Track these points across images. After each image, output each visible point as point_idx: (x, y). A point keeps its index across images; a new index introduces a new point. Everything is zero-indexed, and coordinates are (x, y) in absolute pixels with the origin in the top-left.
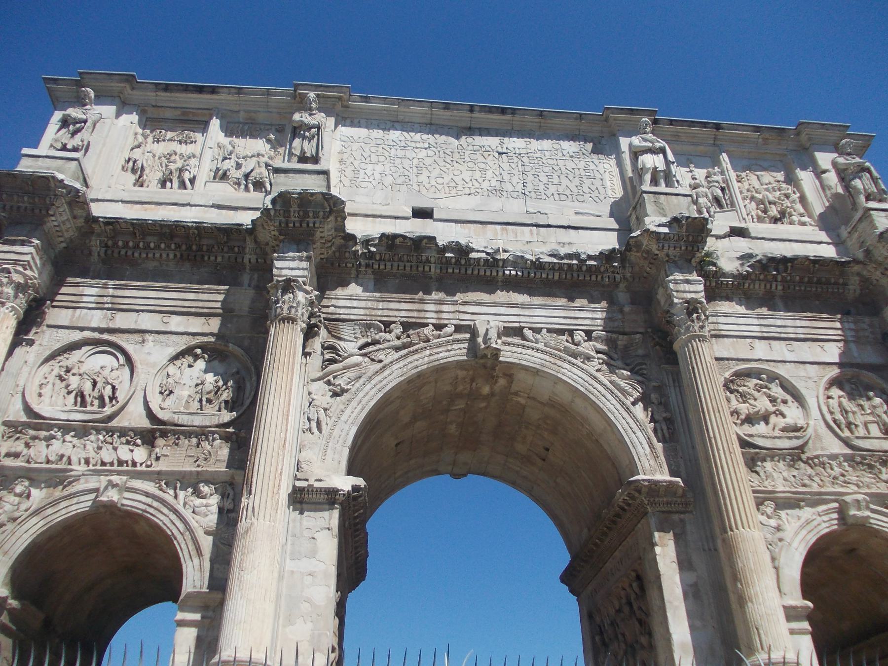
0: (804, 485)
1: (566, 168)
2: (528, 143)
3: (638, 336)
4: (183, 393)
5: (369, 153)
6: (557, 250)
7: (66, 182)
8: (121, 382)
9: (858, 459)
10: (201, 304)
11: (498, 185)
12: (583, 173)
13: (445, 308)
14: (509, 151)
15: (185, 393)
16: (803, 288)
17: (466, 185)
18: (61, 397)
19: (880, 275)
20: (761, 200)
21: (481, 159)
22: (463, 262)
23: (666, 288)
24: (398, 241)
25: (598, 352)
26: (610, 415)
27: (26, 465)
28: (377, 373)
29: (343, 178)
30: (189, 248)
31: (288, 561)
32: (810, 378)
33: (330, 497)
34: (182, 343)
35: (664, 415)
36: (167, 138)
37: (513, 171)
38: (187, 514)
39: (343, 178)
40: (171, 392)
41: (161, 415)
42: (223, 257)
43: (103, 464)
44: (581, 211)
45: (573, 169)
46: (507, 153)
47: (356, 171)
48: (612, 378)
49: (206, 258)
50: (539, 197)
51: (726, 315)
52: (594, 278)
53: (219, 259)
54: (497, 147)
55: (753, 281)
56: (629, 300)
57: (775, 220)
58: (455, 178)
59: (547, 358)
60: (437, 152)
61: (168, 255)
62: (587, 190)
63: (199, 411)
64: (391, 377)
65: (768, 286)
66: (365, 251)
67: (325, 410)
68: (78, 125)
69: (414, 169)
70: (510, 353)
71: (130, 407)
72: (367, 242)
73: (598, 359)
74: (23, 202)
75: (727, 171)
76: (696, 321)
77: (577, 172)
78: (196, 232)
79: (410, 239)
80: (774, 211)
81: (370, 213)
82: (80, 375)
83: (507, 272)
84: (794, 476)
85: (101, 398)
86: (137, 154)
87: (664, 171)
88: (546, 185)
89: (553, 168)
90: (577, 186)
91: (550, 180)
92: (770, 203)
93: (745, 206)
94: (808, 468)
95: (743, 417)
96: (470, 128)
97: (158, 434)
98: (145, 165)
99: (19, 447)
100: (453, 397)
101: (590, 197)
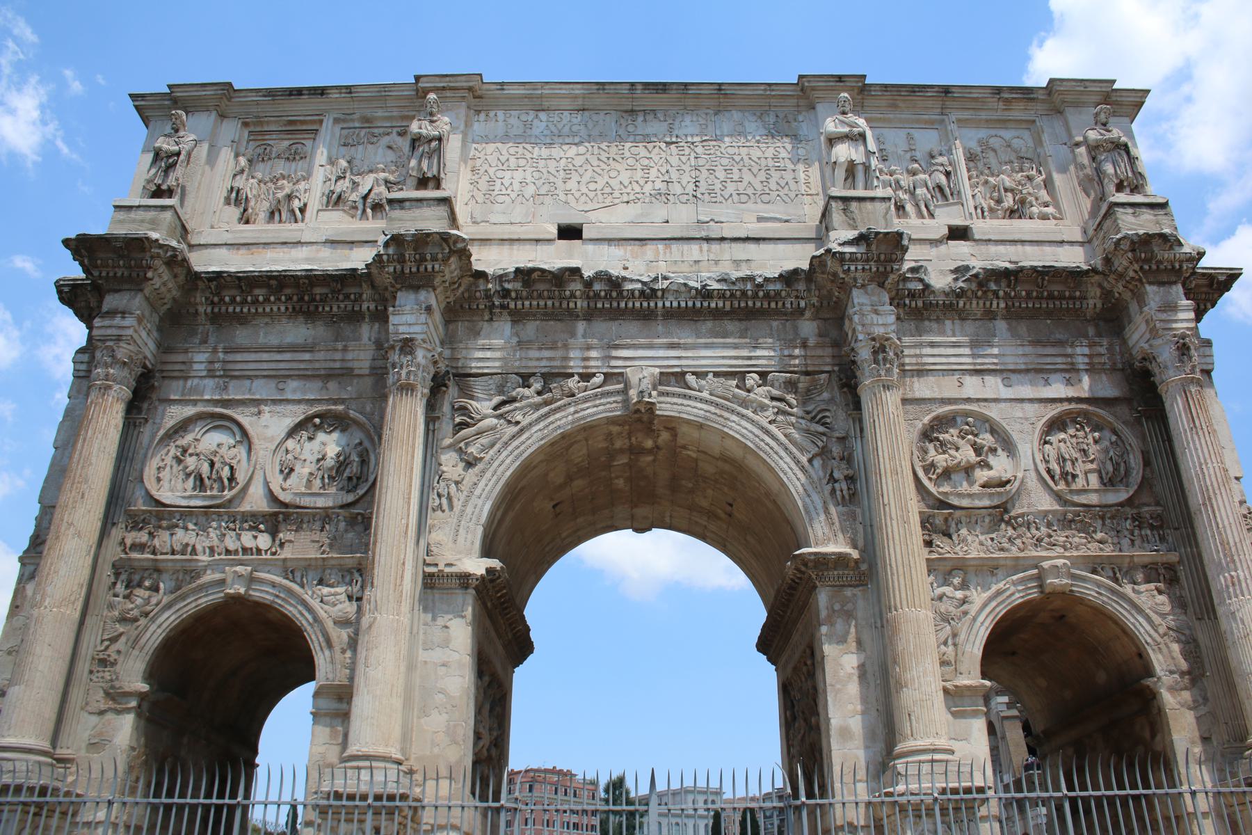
0: (1002, 549)
3: (823, 376)
4: (303, 471)
5: (507, 156)
6: (727, 274)
7: (161, 242)
8: (239, 461)
9: (1070, 516)
10: (317, 365)
11: (663, 186)
12: (771, 163)
13: (594, 354)
15: (306, 471)
16: (1030, 305)
17: (624, 191)
18: (180, 480)
19: (1121, 288)
20: (995, 186)
21: (643, 153)
22: (614, 294)
23: (851, 320)
24: (535, 275)
25: (773, 399)
26: (782, 475)
27: (152, 556)
28: (513, 437)
29: (476, 193)
30: (301, 299)
31: (421, 651)
32: (1026, 419)
33: (464, 579)
34: (299, 413)
35: (846, 472)
36: (273, 156)
37: (684, 167)
38: (315, 604)
39: (476, 193)
40: (292, 470)
41: (284, 497)
42: (339, 307)
43: (228, 552)
44: (766, 215)
45: (759, 158)
47: (491, 181)
48: (789, 431)
49: (320, 309)
50: (714, 200)
51: (932, 345)
52: (773, 305)
53: (335, 309)
55: (970, 300)
56: (816, 331)
57: (1012, 213)
58: (611, 181)
59: (712, 409)
60: (590, 148)
61: (279, 309)
63: (322, 491)
64: (530, 441)
65: (988, 304)
66: (498, 288)
67: (457, 483)
68: (171, 161)
69: (562, 172)
70: (668, 407)
71: (252, 490)
72: (501, 278)
73: (773, 407)
74: (119, 267)
76: (881, 362)
77: (763, 162)
78: (307, 281)
79: (550, 272)
80: (1009, 201)
81: (506, 237)
82: (197, 455)
83: (668, 304)
84: (992, 539)
85: (220, 479)
86: (240, 182)
87: (863, 164)
91: (729, 176)
92: (1006, 190)
93: (973, 196)
94: (1009, 528)
95: (939, 471)
96: (632, 111)
97: (281, 516)
98: (250, 196)
99: (143, 537)
100: (612, 454)
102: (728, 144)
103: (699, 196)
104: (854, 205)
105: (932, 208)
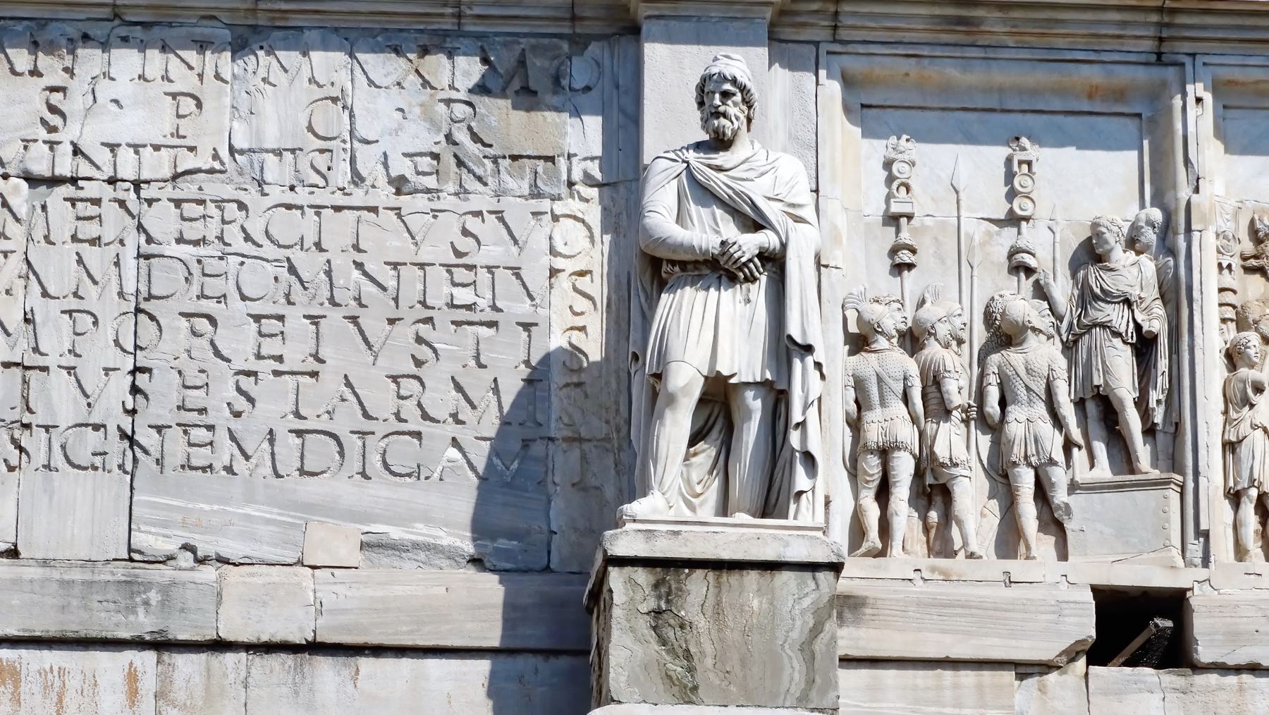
1: (359, 266)
2: (188, 105)
12: (440, 291)
14: (85, 169)
44: (396, 533)
46: (74, 181)
50: (200, 457)
54: (27, 143)
62: (441, 399)
75: (1189, 230)
87: (765, 384)
88: (247, 383)
89: (292, 270)
90: (395, 379)
91: (270, 347)
93: (1231, 447)
101: (455, 444)
102: (277, 194)
103: (146, 437)
104: (698, 585)
105: (1060, 496)
